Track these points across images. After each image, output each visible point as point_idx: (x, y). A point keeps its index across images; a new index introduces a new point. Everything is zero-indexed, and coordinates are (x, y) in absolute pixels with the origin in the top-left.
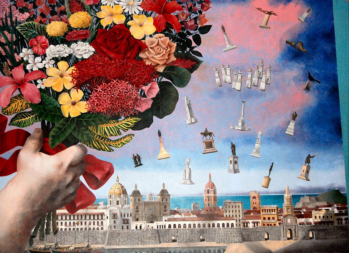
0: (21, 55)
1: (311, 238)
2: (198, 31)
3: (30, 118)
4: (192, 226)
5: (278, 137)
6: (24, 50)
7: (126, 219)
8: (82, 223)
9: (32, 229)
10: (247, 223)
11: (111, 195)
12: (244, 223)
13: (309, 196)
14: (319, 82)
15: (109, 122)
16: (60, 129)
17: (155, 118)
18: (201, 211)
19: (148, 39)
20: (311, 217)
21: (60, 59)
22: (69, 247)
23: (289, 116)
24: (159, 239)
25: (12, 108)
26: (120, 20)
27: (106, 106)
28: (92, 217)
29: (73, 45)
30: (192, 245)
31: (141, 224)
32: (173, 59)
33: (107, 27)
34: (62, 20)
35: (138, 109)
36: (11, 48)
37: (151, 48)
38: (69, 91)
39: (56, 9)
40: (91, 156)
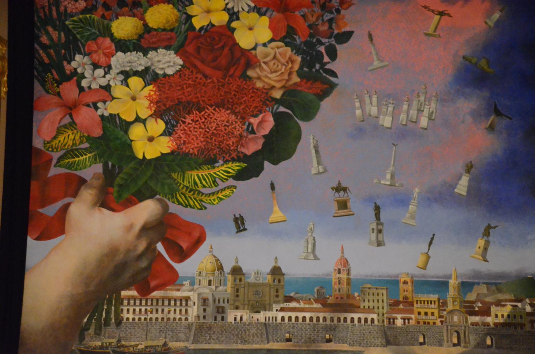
0: (74, 64)
1: (489, 347)
2: (333, 39)
3: (86, 158)
4: (315, 320)
5: (442, 196)
6: (78, 57)
8: (157, 310)
10: (394, 319)
11: (200, 272)
12: (389, 319)
14: (510, 119)
15: (200, 168)
17: (266, 163)
18: (328, 298)
19: (260, 49)
21: (131, 73)
22: (137, 345)
23: (460, 166)
24: (267, 337)
26: (220, 18)
27: (198, 144)
28: (172, 303)
29: (151, 54)
30: (313, 347)
31: (241, 314)
32: (296, 79)
33: (201, 29)
34: (134, 16)
36: (57, 52)
37: (264, 63)
38: (144, 122)
40: (174, 216)
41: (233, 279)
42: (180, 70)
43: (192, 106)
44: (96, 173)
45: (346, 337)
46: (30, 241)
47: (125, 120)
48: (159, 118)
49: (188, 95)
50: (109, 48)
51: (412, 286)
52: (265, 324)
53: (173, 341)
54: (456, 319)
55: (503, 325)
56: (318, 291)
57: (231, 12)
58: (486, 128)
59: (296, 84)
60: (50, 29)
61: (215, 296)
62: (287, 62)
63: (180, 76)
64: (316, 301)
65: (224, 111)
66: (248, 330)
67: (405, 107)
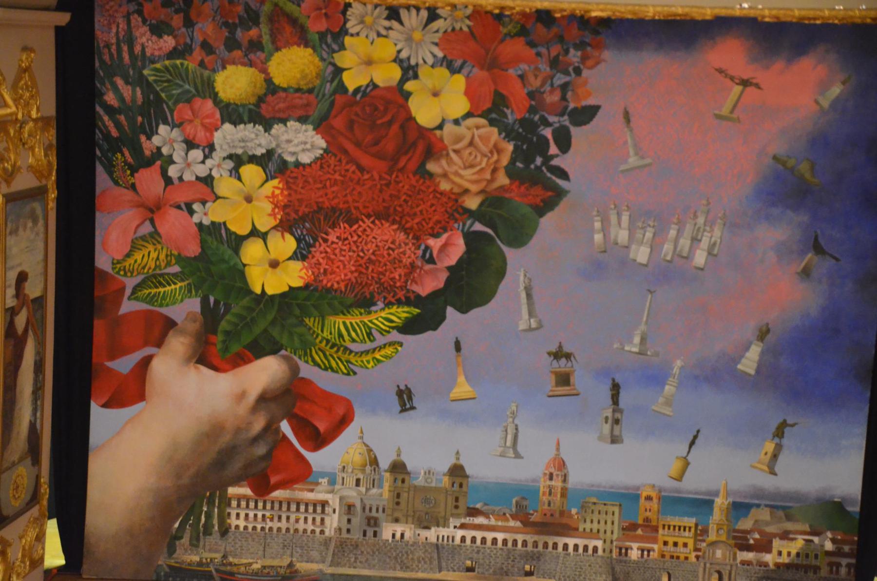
0: (156, 140)
2: (566, 117)
3: (176, 289)
4: (510, 544)
5: (717, 374)
6: (163, 129)
7: (373, 517)
8: (280, 518)
9: (175, 522)
10: (627, 549)
11: (344, 467)
12: (620, 549)
13: (772, 507)
15: (349, 313)
16: (242, 318)
17: (450, 310)
18: (532, 515)
19: (449, 128)
20: (769, 550)
21: (245, 158)
22: (251, 564)
23: (750, 329)
24: (439, 562)
25: (136, 261)
26: (387, 75)
27: (346, 275)
28: (302, 508)
29: (277, 129)
31: (403, 529)
32: (503, 180)
33: (357, 90)
34: (251, 64)
35: (416, 288)
36: (132, 120)
37: (455, 151)
38: (264, 236)
39: (239, 33)
41: (392, 480)
42: (322, 157)
43: (339, 216)
44: (191, 312)
45: (555, 570)
46: (96, 411)
47: (235, 233)
48: (287, 231)
49: (333, 198)
50: (211, 116)
51: (659, 504)
52: (437, 545)
53: (302, 562)
54: (719, 553)
55: (788, 566)
56: (517, 502)
57: (405, 65)
58: (798, 273)
59: (502, 188)
60: (119, 82)
61: (366, 501)
62: (491, 152)
63: (322, 167)
64: (514, 517)
65: (387, 225)
66: (412, 552)
67: (673, 233)
